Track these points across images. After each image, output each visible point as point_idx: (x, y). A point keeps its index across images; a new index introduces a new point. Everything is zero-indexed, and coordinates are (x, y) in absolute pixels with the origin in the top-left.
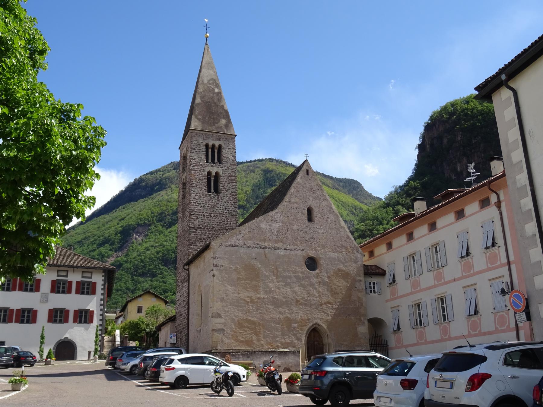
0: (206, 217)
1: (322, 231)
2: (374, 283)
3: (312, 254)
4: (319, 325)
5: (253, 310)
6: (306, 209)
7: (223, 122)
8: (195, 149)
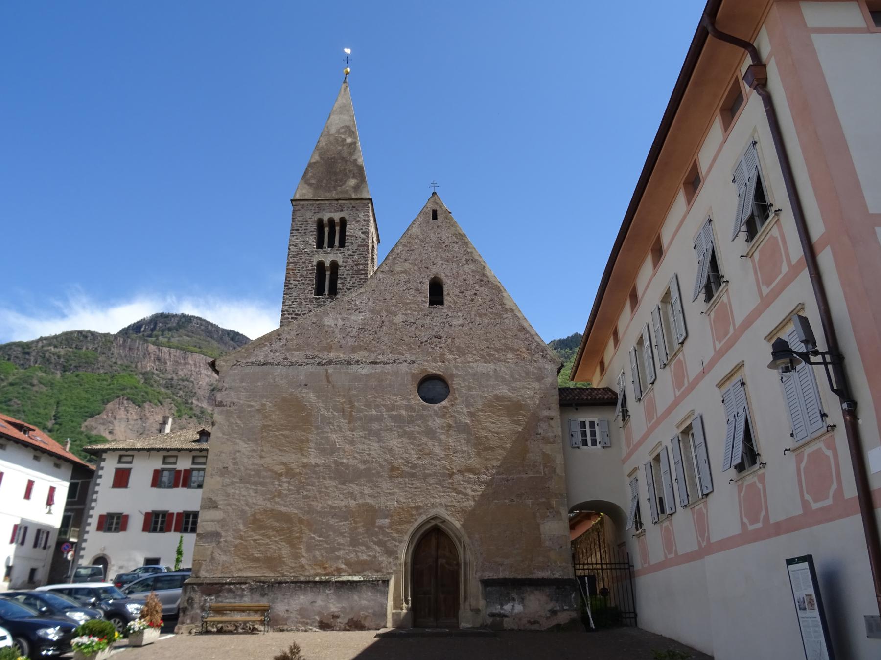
1: (461, 321)
2: (592, 424)
3: (434, 368)
4: (444, 521)
5: (289, 490)
6: (427, 282)
7: (352, 182)
8: (297, 230)
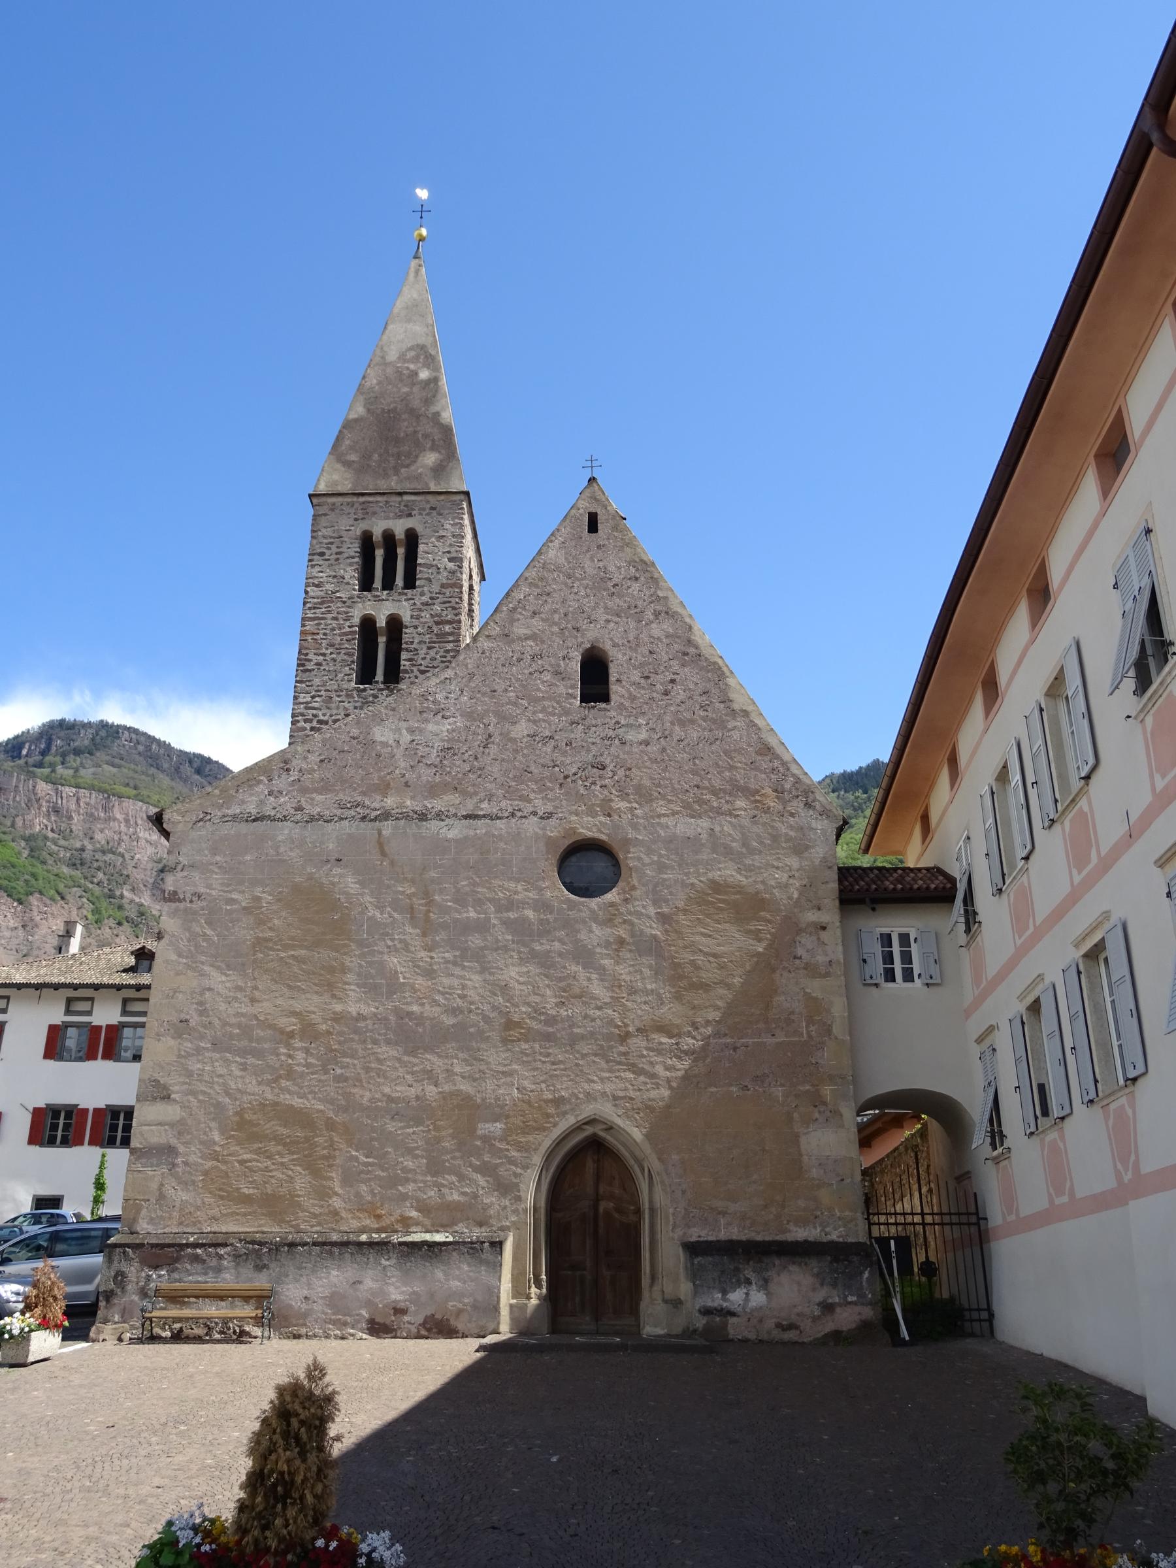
1: (643, 735)
2: (905, 939)
3: (589, 827)
4: (610, 1128)
5: (308, 1065)
7: (430, 458)
8: (322, 554)
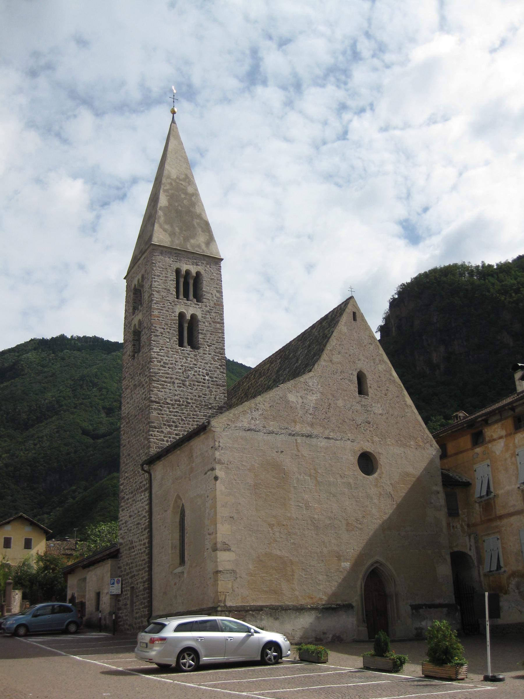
0: (176, 385)
1: (381, 412)
3: (368, 447)
4: (381, 564)
6: (355, 374)
8: (159, 276)
